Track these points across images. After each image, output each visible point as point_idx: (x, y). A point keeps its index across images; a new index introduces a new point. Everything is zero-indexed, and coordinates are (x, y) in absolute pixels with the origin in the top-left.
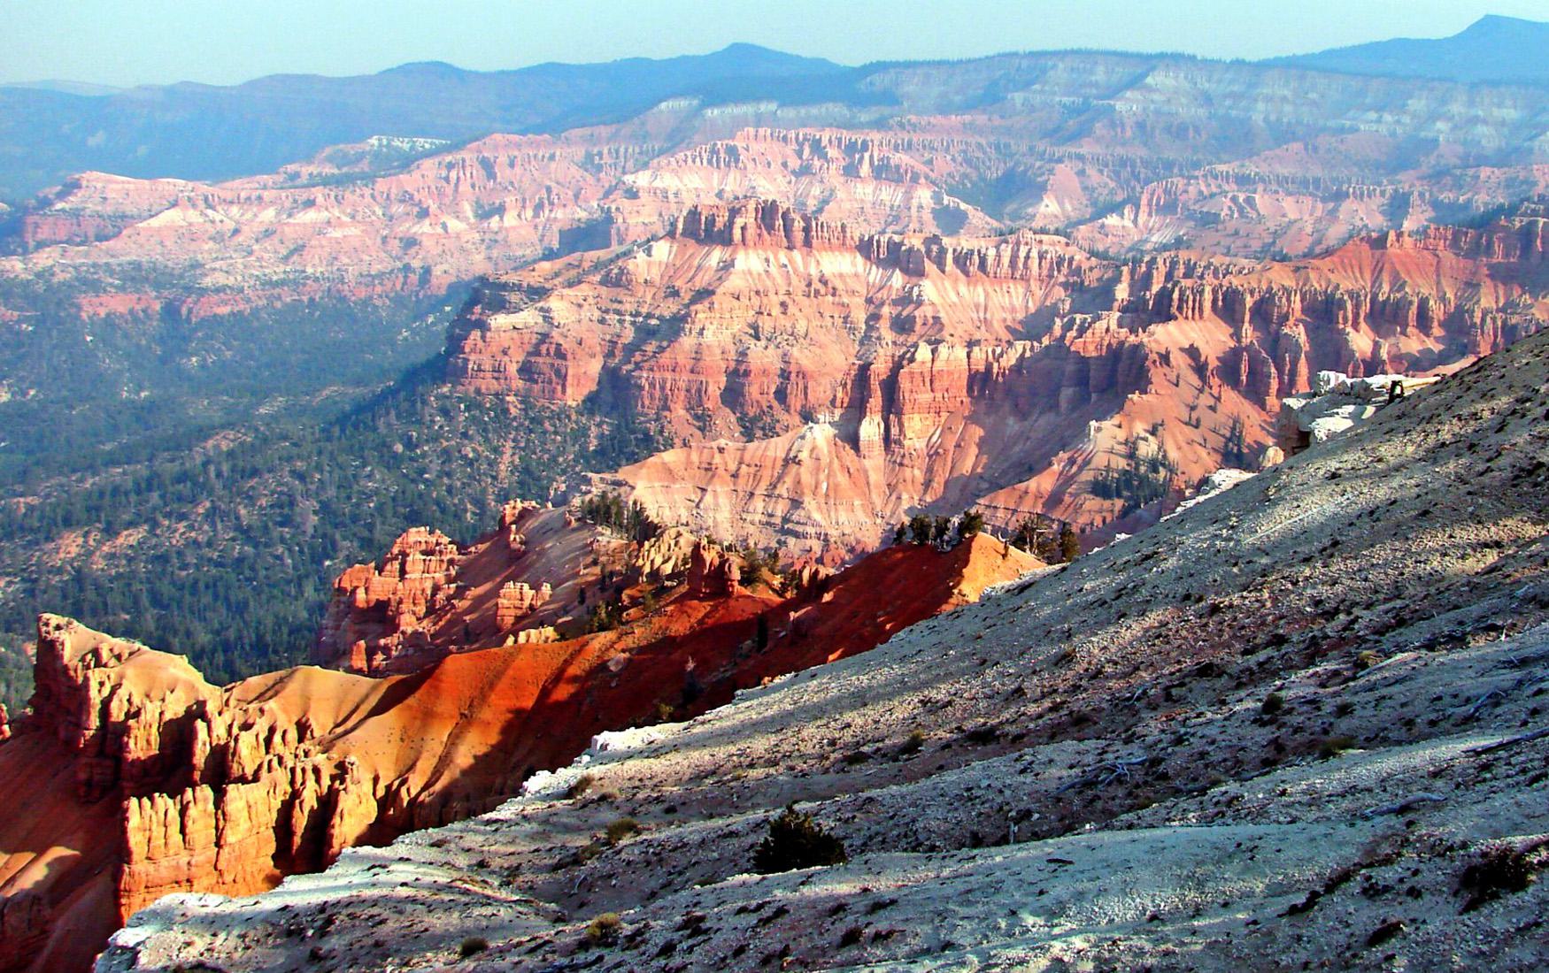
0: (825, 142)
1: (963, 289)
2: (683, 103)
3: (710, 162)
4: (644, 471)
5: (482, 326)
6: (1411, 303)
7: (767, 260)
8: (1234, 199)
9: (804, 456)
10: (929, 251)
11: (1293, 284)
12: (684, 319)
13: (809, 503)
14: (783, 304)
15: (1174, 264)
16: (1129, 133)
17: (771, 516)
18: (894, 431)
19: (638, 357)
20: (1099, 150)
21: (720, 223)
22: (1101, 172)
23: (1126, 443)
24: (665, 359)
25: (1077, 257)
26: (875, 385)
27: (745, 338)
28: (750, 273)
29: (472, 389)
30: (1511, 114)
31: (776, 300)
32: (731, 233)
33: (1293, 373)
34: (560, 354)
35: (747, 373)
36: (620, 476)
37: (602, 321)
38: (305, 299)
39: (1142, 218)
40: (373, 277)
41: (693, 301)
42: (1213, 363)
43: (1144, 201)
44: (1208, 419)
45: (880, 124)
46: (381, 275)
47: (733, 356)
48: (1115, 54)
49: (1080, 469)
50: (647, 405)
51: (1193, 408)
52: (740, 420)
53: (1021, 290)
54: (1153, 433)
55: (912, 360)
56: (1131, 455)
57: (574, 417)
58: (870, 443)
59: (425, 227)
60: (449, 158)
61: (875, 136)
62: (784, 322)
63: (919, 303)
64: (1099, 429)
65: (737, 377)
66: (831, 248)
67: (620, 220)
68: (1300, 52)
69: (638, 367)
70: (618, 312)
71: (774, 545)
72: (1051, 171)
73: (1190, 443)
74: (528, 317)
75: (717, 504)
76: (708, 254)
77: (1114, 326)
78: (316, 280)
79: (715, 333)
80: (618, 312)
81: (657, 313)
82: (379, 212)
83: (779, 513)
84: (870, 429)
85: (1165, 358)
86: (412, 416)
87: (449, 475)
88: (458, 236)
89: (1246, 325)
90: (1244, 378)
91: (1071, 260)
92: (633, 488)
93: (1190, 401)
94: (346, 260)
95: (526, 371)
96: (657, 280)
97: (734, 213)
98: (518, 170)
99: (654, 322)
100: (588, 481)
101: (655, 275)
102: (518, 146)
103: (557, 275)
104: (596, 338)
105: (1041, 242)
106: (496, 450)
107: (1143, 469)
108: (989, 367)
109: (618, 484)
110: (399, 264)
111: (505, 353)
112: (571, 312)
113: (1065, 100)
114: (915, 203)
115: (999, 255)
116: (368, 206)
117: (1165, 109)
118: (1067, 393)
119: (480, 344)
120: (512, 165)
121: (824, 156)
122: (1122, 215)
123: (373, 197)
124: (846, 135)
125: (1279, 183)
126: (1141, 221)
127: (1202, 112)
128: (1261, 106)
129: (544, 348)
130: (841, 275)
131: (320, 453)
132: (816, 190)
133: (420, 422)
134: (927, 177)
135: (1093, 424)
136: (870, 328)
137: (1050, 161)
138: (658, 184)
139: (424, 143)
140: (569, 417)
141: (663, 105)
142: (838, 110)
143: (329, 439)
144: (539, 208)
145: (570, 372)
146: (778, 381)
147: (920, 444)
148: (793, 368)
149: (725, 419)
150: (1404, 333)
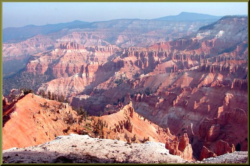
0: (85, 33)
1: (101, 54)
2: (66, 29)
3: (69, 37)
4: (50, 83)
5: (30, 63)
6: (164, 53)
7: (72, 51)
8: (144, 39)
9: (74, 79)
10: (96, 48)
11: (146, 51)
12: (59, 60)
13: (75, 86)
14: (74, 57)
15: (132, 48)
16: (130, 30)
17: (69, 88)
18: (87, 75)
19: (53, 66)
20: (126, 33)
21: (65, 45)
22: (125, 36)
23: (120, 75)
24: (57, 66)
25: (118, 48)
26: (84, 68)
27: (69, 62)
28: (69, 53)
29: (28, 72)
30: (184, 25)
31: (73, 56)
32: (66, 48)
33: (146, 64)
34: (41, 66)
35: (69, 67)
36: (47, 84)
37: (48, 61)
38: (10, 60)
39: (131, 43)
40: (20, 56)
41: (61, 57)
42: (134, 63)
43: (132, 40)
44: (133, 71)
45: (94, 31)
46: (21, 56)
47: (67, 65)
48: (128, 19)
49: (114, 79)
50: (54, 73)
51: (131, 70)
52: (68, 74)
53: (110, 53)
54: (125, 73)
55: (90, 64)
56: (121, 77)
57: (44, 75)
58: (84, 77)
59: (28, 49)
60: (31, 38)
61: (93, 32)
62: (74, 60)
63: (94, 56)
64: (116, 73)
65: (67, 68)
66: (82, 49)
67: (55, 46)
68: (156, 18)
69: (53, 67)
70: (50, 59)
71: (70, 93)
72: (118, 36)
73: (130, 75)
74: (37, 61)
75: (61, 87)
76: (63, 51)
77: (119, 58)
78: (12, 57)
79: (64, 62)
80: (50, 59)
81: (56, 59)
82: (21, 47)
83: (70, 88)
84: (84, 75)
85: (127, 62)
86: (19, 76)
87: (25, 85)
88: (33, 50)
89: (139, 57)
90: (139, 65)
91: (117, 49)
92: (48, 85)
93: (130, 69)
94: (16, 54)
95: (36, 69)
96: (56, 54)
97: (67, 44)
98: (42, 40)
99: (55, 61)
100: (42, 85)
101: (55, 54)
102: (42, 36)
103: (42, 54)
104: (47, 63)
105: (112, 46)
106: (32, 81)
107: (123, 79)
108: (101, 65)
109: (46, 85)
110: (24, 54)
111: (33, 66)
112: (43, 60)
113: (121, 26)
114: (99, 42)
115: (106, 48)
116: (20, 46)
117: (135, 27)
118: (113, 68)
119: (29, 65)
120: (41, 39)
121: (85, 36)
122: (128, 42)
123: (20, 45)
124: (89, 33)
125: (151, 37)
126: (131, 43)
127: (140, 27)
128: (149, 26)
129: (39, 65)
130: (83, 52)
131: (6, 82)
132: (84, 41)
133: (21, 77)
134: (100, 38)
135: (116, 73)
136: (87, 60)
137: (118, 35)
138: (61, 41)
139: (29, 36)
140: (43, 75)
141: (63, 29)
142: (89, 29)
143: (7, 80)
144: (45, 45)
145: (43, 69)
146: (73, 68)
147: (92, 77)
148: (76, 67)
149: (66, 74)
150: (163, 57)
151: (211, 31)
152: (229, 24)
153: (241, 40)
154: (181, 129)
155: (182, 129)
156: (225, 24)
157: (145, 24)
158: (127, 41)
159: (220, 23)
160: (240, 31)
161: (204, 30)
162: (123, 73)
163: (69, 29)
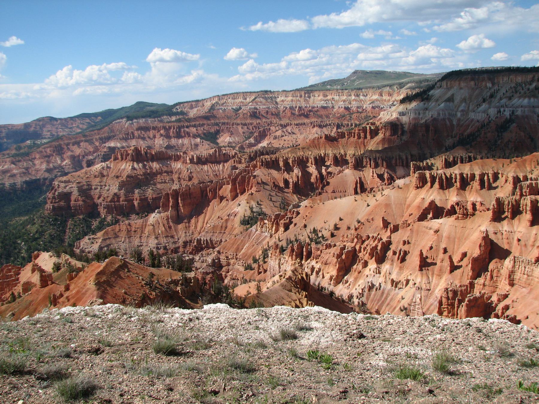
113: (234, 107)
151: (425, 104)
152: (461, 88)
153: (490, 117)
154: (398, 308)
155: (400, 308)
156: (452, 87)
157: (283, 101)
158: (249, 138)
159: (441, 87)
160: (484, 101)
161: (410, 104)
162: (254, 204)
163: (128, 120)
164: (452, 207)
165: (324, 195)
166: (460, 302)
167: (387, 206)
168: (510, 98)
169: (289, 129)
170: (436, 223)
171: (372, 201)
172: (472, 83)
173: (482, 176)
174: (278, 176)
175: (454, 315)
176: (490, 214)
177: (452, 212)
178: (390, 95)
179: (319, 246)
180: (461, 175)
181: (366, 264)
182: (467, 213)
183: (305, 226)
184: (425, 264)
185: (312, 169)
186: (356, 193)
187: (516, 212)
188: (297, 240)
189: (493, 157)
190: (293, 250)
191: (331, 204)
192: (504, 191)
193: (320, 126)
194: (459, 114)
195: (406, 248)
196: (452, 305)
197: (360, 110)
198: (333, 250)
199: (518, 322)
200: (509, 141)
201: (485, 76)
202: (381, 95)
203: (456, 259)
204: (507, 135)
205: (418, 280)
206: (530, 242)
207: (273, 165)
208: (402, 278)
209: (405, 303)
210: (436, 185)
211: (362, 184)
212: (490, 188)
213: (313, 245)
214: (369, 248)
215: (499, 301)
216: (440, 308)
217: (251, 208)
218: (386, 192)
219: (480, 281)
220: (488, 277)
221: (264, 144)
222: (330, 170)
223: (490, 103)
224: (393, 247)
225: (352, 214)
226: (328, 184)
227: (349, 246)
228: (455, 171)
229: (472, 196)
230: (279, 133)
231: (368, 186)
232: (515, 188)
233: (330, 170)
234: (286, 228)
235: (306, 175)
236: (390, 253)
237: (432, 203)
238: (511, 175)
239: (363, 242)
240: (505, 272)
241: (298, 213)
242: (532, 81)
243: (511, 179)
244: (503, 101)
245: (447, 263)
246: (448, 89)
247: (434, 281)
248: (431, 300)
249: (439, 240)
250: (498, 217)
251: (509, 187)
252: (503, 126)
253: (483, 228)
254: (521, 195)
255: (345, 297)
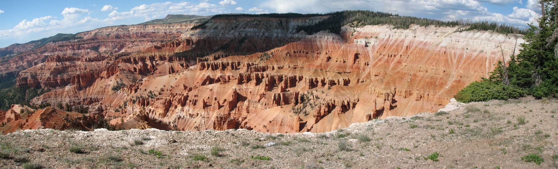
156: (216, 22)
160: (232, 29)
162: (119, 80)
164: (218, 78)
165: (155, 74)
166: (224, 122)
167: (186, 79)
168: (244, 28)
169: (136, 43)
170: (210, 86)
171: (178, 77)
172: (227, 21)
173: (232, 64)
174: (131, 66)
175: (221, 128)
176: (237, 80)
177: (218, 80)
178: (186, 26)
179: (153, 99)
180: (222, 63)
181: (176, 107)
182: (225, 81)
183: (146, 90)
184: (206, 105)
185: (148, 62)
186: (170, 73)
187: (249, 79)
188: (141, 97)
189: (237, 55)
190: (139, 102)
191: (158, 79)
192: (243, 70)
193: (152, 42)
194: (220, 35)
195: (196, 98)
196: (220, 124)
197: (171, 34)
198: (160, 101)
199: (252, 129)
200: (245, 47)
201: (233, 17)
202: (181, 26)
203: (221, 103)
204: (243, 45)
205: (203, 113)
206: (256, 93)
207: (128, 61)
208: (195, 113)
209: (197, 125)
210: (210, 68)
211: (172, 69)
212: (236, 69)
213: (150, 99)
214: (177, 99)
215: (243, 120)
216: (214, 126)
217: (117, 82)
218: (185, 72)
219: (233, 112)
220: (237, 110)
221: (123, 51)
222: (157, 62)
223: (235, 30)
224: (189, 98)
225: (168, 83)
226: (157, 69)
227: (168, 98)
228: (219, 61)
229: (228, 73)
230: (130, 45)
231: (176, 70)
232: (248, 69)
233: (157, 62)
234: (136, 91)
235: (145, 65)
236: (188, 101)
237: (208, 77)
238: (246, 63)
239: (174, 96)
240: (245, 107)
241: (142, 84)
242: (254, 20)
243: (246, 65)
244: (241, 29)
245: (217, 105)
246: (215, 23)
247: (211, 113)
248: (210, 122)
249: (213, 94)
250: (240, 82)
251: (245, 68)
252: (242, 41)
253: (234, 88)
254: (251, 72)
255: (168, 123)
